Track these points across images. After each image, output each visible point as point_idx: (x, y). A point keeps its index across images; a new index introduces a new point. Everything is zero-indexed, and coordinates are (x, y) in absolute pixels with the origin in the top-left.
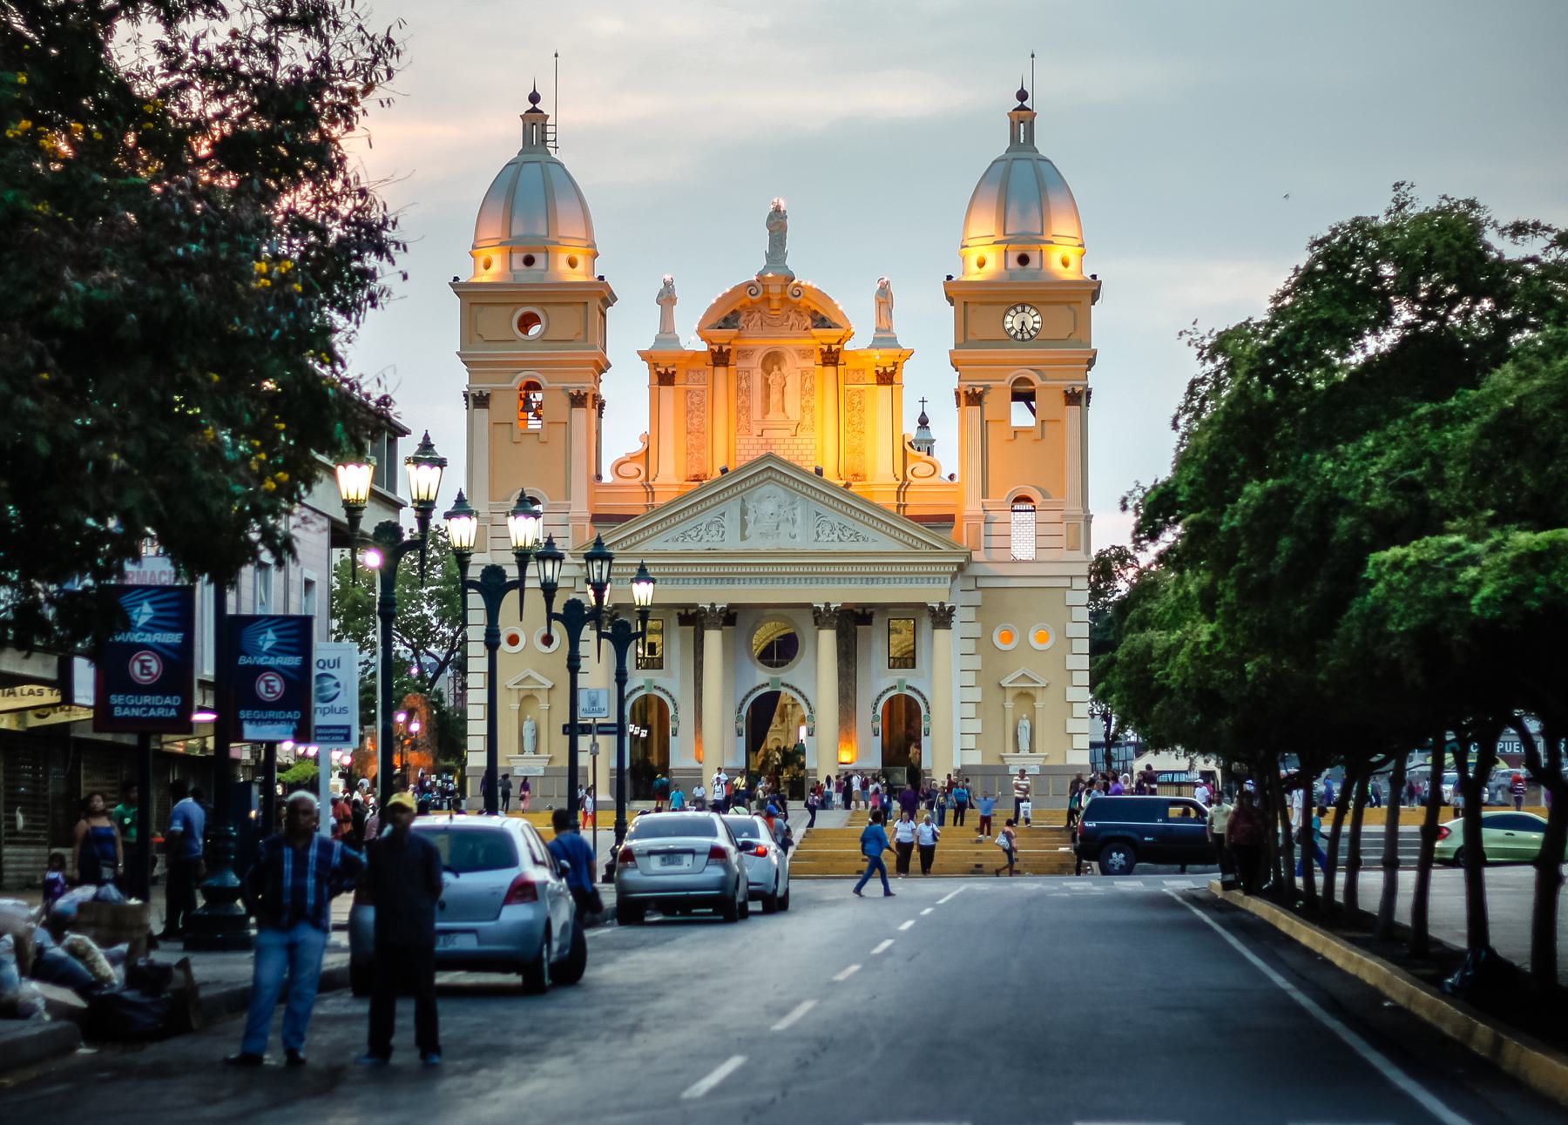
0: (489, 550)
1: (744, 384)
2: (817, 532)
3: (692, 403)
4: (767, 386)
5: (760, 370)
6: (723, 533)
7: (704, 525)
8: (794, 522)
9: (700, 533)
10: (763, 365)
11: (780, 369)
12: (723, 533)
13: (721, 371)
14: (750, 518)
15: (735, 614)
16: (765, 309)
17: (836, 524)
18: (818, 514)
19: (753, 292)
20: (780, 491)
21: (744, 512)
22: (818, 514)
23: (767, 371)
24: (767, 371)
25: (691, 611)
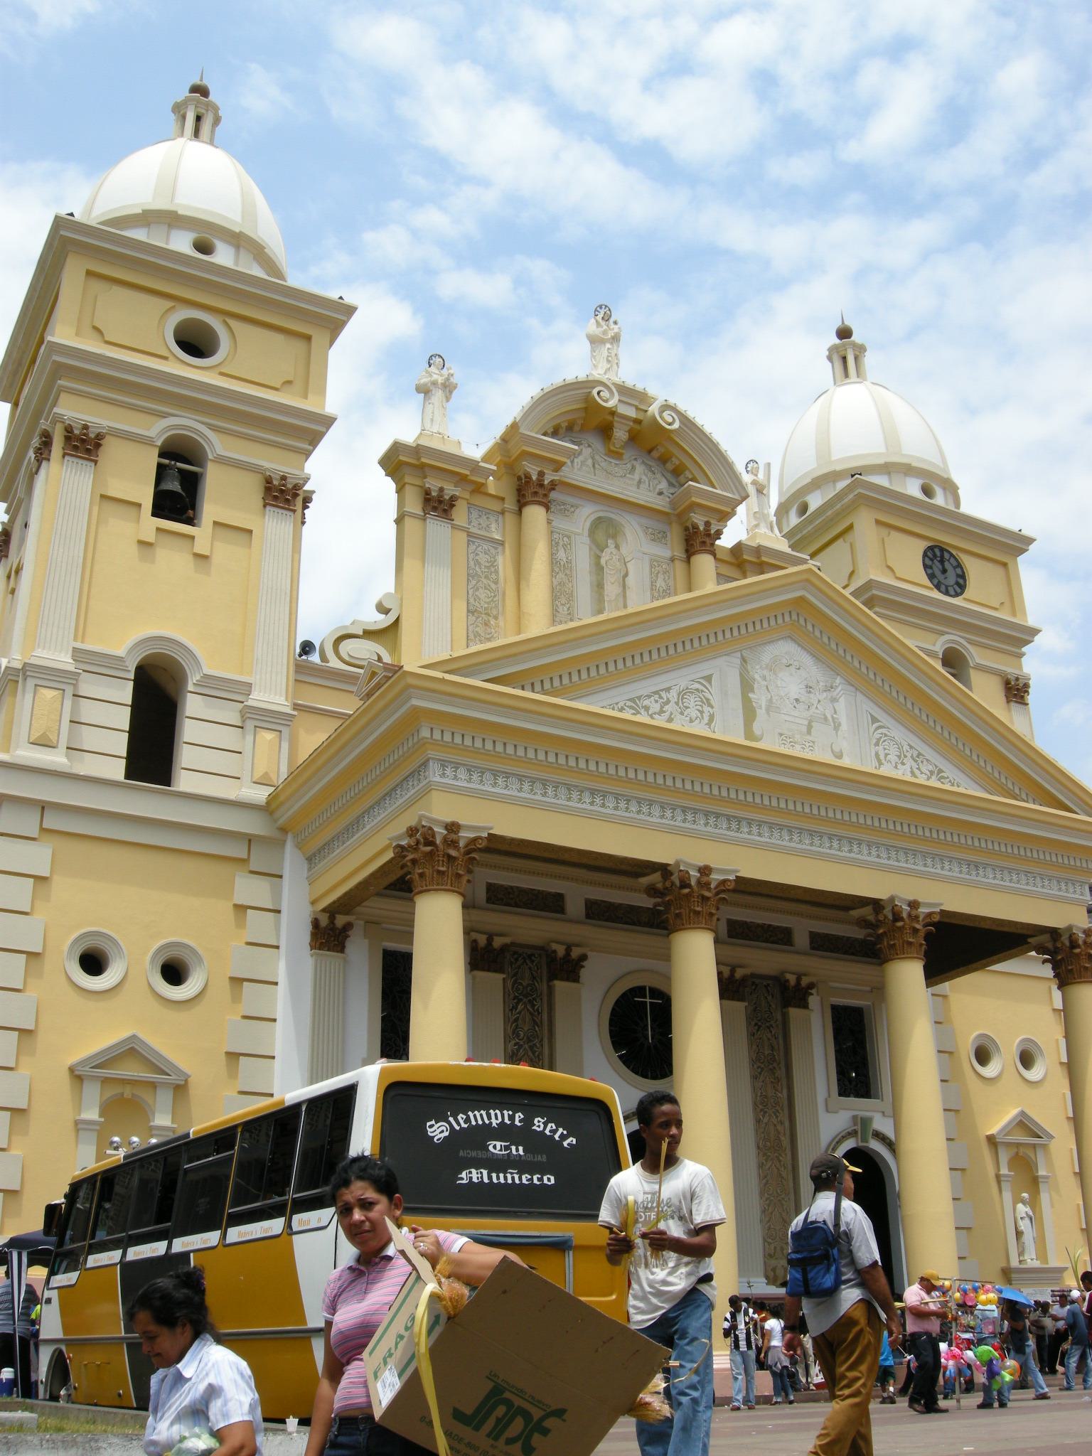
0: (63, 743)
1: (561, 555)
2: (877, 755)
3: (477, 563)
4: (598, 569)
5: (587, 540)
6: (712, 717)
7: (675, 694)
8: (837, 727)
9: (666, 708)
10: (592, 532)
11: (617, 547)
12: (712, 717)
13: (535, 513)
14: (759, 698)
15: (583, 957)
16: (597, 444)
17: (906, 747)
18: (874, 720)
19: (601, 393)
20: (807, 660)
21: (747, 686)
22: (874, 720)
23: (602, 551)
24: (598, 548)
25: (498, 942)
